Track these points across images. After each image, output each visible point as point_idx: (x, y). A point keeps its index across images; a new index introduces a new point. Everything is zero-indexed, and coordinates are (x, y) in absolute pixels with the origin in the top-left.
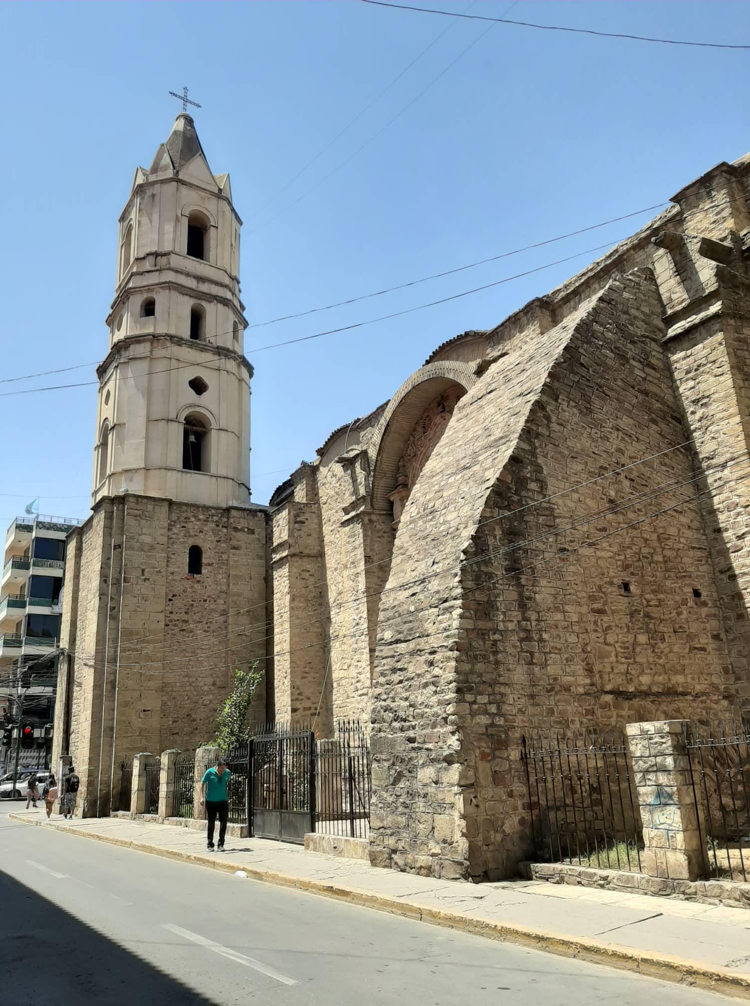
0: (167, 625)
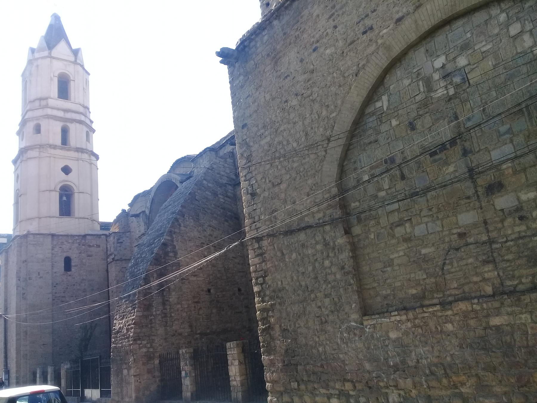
0: (53, 300)
